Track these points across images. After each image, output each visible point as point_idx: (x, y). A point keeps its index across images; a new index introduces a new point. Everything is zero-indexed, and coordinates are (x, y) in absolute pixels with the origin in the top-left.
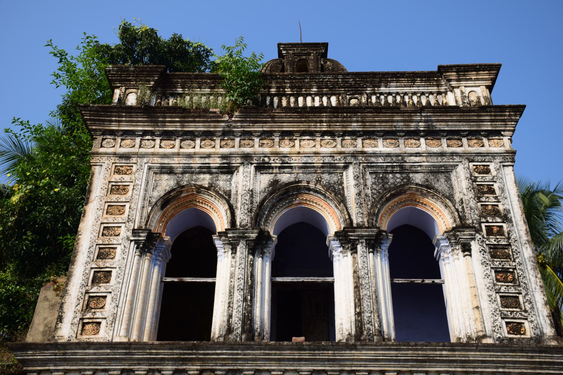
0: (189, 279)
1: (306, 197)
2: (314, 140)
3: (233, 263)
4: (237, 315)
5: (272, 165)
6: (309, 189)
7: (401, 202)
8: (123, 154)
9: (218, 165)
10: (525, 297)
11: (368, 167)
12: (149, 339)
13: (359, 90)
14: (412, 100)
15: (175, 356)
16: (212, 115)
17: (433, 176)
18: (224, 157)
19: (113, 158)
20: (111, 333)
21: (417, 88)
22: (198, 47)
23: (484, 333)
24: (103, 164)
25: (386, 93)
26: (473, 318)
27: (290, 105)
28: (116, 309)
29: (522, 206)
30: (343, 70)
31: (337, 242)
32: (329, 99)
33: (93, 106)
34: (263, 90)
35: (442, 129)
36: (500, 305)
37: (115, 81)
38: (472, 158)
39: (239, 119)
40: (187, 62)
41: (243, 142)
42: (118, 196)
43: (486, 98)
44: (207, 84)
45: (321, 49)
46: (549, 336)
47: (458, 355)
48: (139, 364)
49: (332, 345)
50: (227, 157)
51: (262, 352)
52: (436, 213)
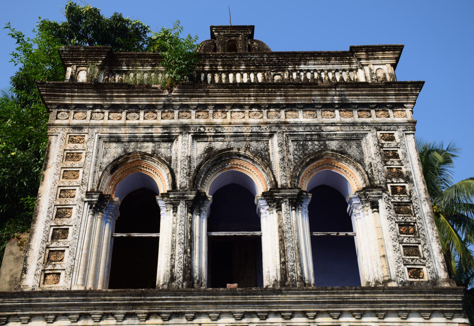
0: (136, 235)
1: (236, 162)
2: (243, 112)
3: (174, 220)
4: (179, 266)
5: (207, 134)
6: (239, 155)
7: (319, 166)
8: (76, 126)
10: (423, 246)
11: (291, 135)
12: (103, 287)
13: (282, 68)
14: (328, 76)
16: (154, 90)
17: (346, 143)
19: (67, 129)
21: (332, 66)
23: (389, 278)
24: (58, 134)
25: (305, 70)
26: (380, 265)
28: (73, 261)
29: (422, 169)
31: (265, 201)
32: (256, 75)
33: (49, 83)
34: (198, 67)
35: (354, 102)
36: (403, 254)
37: (68, 60)
38: (379, 127)
39: (178, 94)
41: (181, 114)
42: (72, 162)
43: (391, 75)
44: (149, 63)
45: (248, 31)
46: (443, 279)
47: (368, 297)
48: (95, 309)
49: (261, 291)
51: (202, 297)
52: (348, 175)
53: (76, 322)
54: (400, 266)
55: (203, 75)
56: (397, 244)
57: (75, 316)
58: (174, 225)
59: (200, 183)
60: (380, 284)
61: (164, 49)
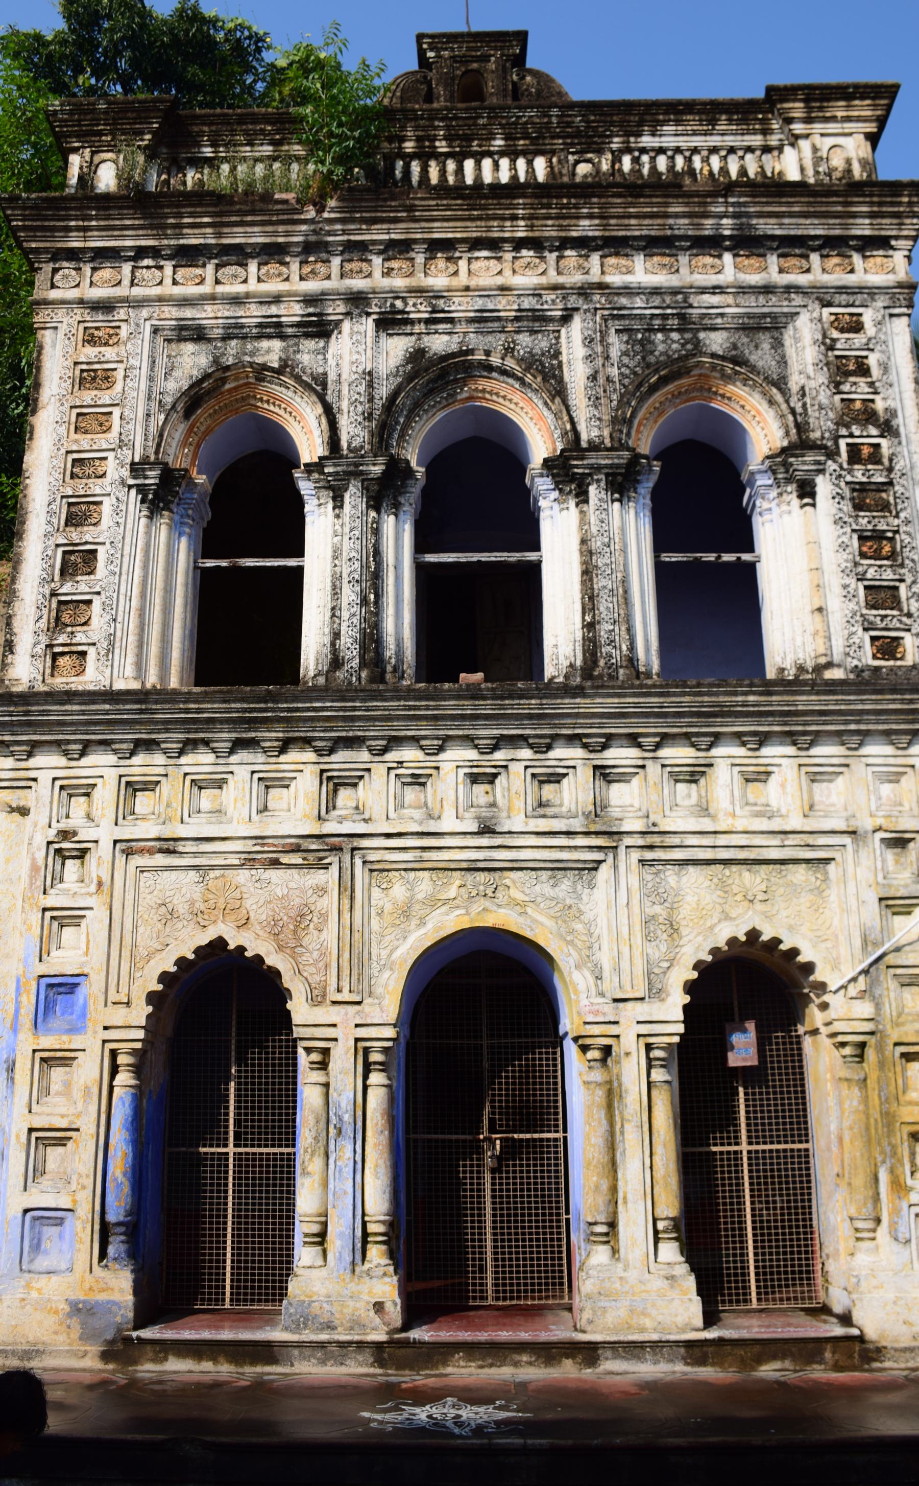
1: (482, 384)
2: (499, 259)
3: (337, 527)
5: (412, 316)
6: (490, 368)
7: (680, 393)
8: (98, 302)
9: (298, 319)
10: (910, 587)
11: (614, 317)
13: (596, 143)
14: (709, 165)
15: (234, 715)
16: (279, 207)
17: (748, 336)
18: (309, 300)
19: (78, 311)
20: (108, 671)
21: (719, 138)
22: (236, 29)
23: (829, 659)
24: (59, 325)
25: (653, 149)
26: (810, 629)
27: (446, 181)
30: (561, 94)
32: (530, 163)
33: (28, 198)
34: (386, 144)
35: (770, 232)
36: (863, 604)
37: (69, 136)
38: (828, 297)
39: (338, 215)
40: (214, 68)
41: (348, 266)
42: (95, 392)
43: (864, 163)
44: (265, 135)
45: (512, 46)
48: (167, 731)
49: (537, 689)
50: (316, 300)
51: (402, 703)
52: (749, 417)
53: (129, 758)
54: (854, 633)
55: (400, 164)
56: (852, 581)
57: (124, 746)
58: (336, 539)
59: (396, 436)
60: (807, 672)
61: (303, 98)
